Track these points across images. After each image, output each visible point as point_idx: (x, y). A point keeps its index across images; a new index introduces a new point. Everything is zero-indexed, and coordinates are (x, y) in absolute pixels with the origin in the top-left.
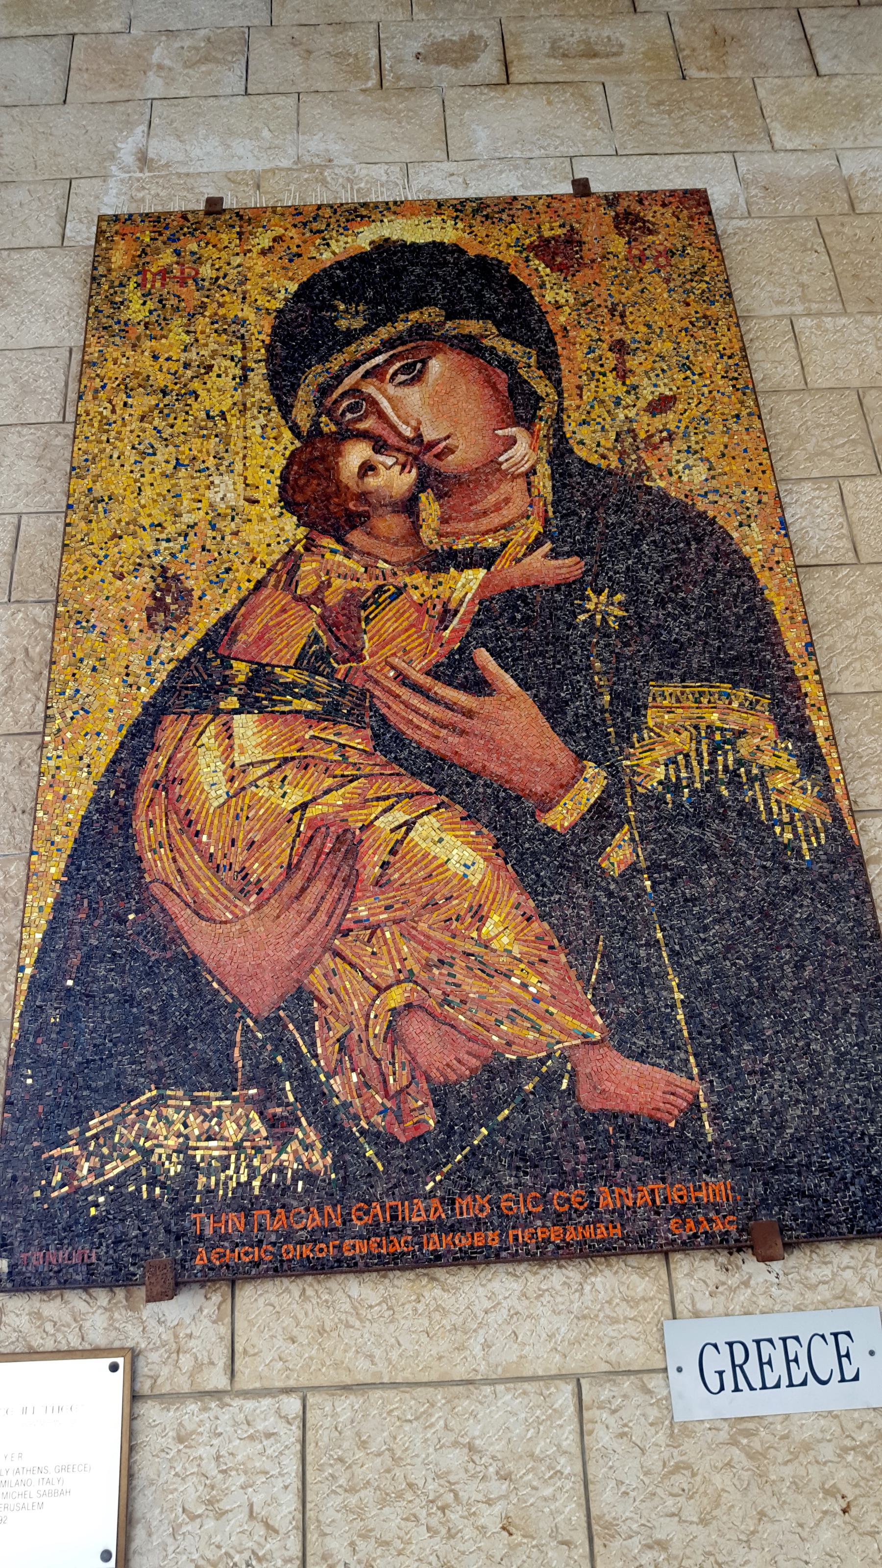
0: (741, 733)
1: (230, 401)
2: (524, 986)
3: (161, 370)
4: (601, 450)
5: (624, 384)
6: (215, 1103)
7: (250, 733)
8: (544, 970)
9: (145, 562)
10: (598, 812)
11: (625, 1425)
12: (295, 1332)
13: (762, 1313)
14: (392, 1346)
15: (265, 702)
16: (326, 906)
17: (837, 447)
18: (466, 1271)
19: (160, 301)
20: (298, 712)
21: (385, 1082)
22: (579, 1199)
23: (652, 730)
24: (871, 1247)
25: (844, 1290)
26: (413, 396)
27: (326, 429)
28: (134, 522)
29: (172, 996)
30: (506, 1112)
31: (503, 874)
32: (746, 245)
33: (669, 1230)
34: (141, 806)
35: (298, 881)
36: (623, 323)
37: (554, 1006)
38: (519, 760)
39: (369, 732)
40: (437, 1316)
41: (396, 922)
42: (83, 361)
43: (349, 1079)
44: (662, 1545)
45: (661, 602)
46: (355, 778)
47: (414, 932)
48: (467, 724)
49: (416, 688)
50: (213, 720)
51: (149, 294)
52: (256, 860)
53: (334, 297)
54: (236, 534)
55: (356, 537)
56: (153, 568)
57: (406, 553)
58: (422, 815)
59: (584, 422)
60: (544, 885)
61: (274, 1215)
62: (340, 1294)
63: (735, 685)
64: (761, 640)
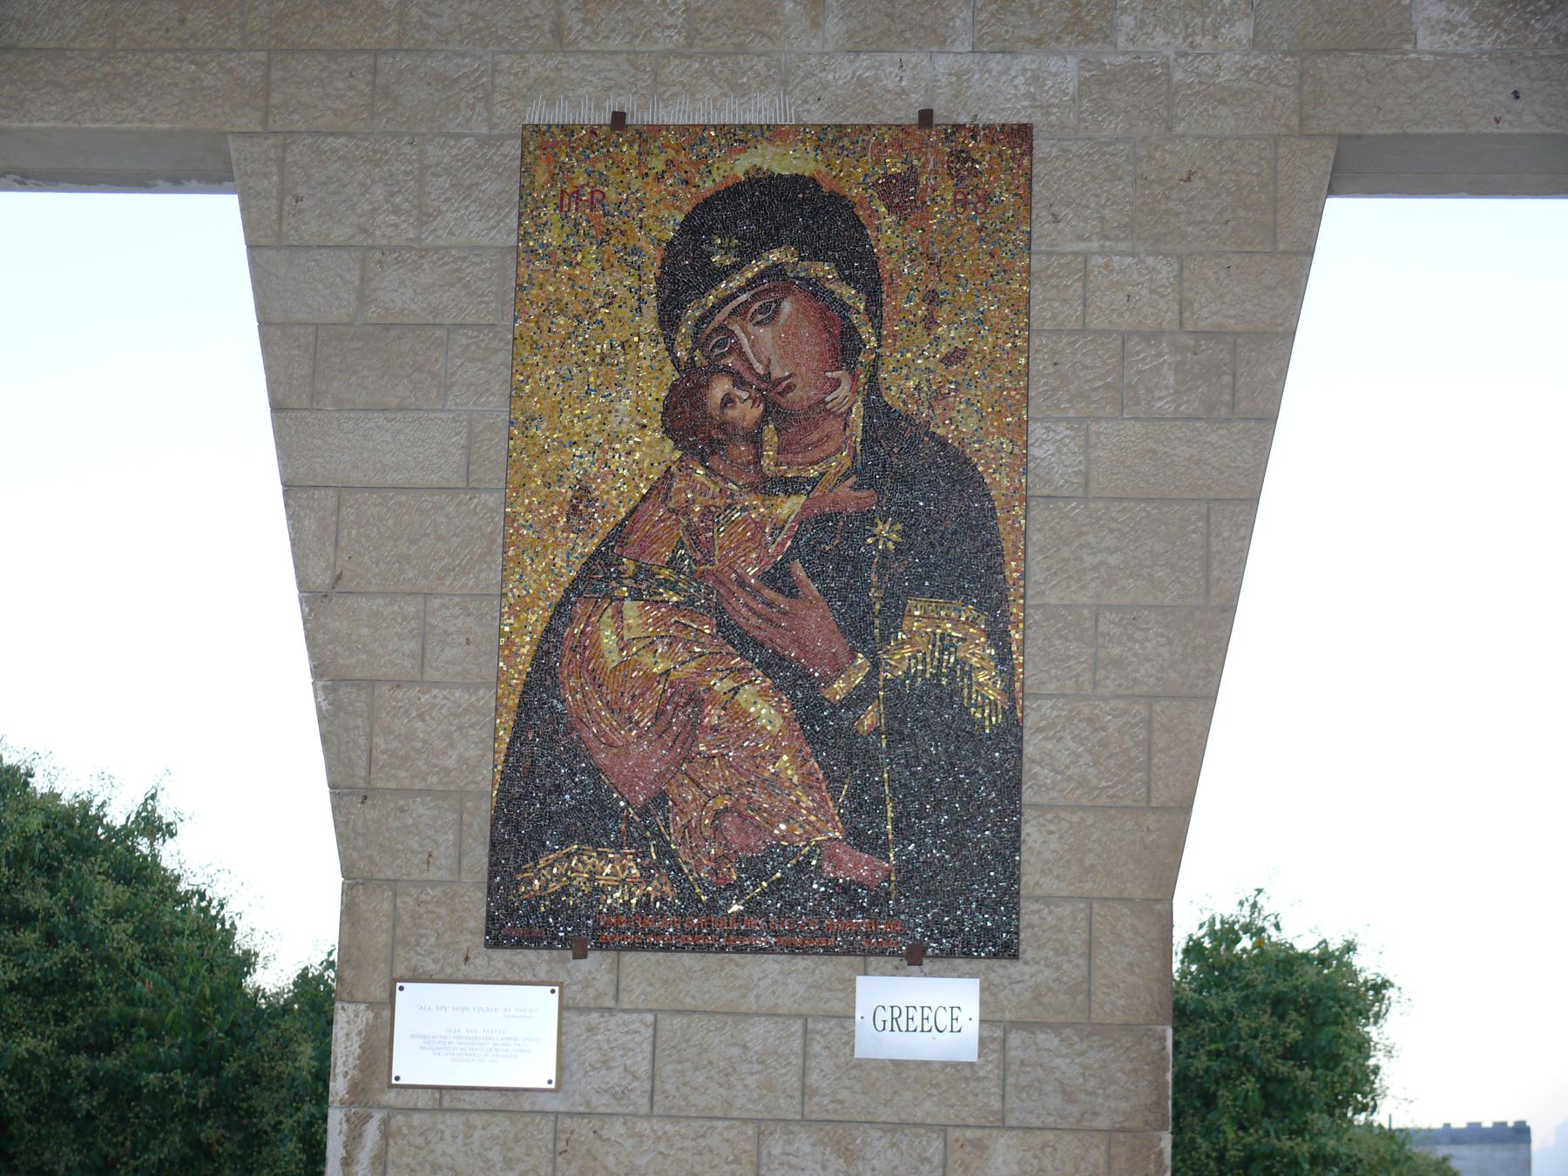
19: (575, 226)
27: (698, 364)
44: (840, 1102)
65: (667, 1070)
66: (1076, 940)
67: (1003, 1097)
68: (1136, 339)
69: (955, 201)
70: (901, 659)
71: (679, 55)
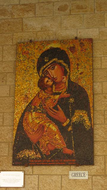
26: (53, 71)
35: (38, 131)
41: (48, 135)
48: (56, 114)
49: (51, 109)
55: (46, 91)
65: (40, 184)
66: (103, 162)
67: (92, 187)
69: (81, 50)
70: (74, 119)
71: (40, 31)
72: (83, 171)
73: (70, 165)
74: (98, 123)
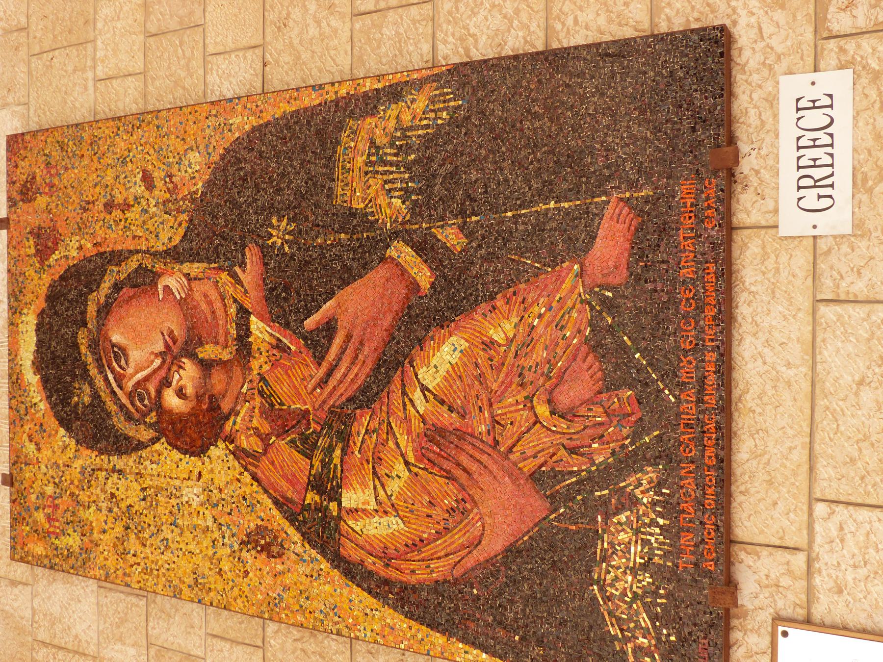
0: (372, 143)
1: (135, 484)
2: (540, 316)
3: (113, 529)
4: (176, 226)
5: (133, 206)
6: (606, 545)
7: (354, 496)
8: (530, 300)
9: (237, 554)
10: (422, 250)
11: (852, 269)
12: (769, 501)
13: (778, 163)
14: (784, 433)
15: (334, 483)
16: (477, 455)
17: (184, 55)
18: (735, 375)
19: (68, 524)
20: (342, 461)
21: (601, 424)
22: (687, 292)
23: (367, 205)
24: (738, 79)
25: (767, 100)
26: (136, 355)
27: (155, 419)
28: (211, 559)
29: (531, 569)
30: (625, 338)
31: (462, 324)
32: (46, 109)
33: (713, 229)
34: (400, 577)
35: (458, 473)
36: (93, 203)
37: (554, 297)
38: (383, 304)
39: (358, 411)
40: (765, 399)
41: (491, 405)
42: (105, 581)
43: (596, 449)
45: (279, 191)
46: (389, 424)
47: (498, 393)
48: (355, 339)
49: (330, 373)
50: (345, 521)
51: (63, 530)
52: (443, 501)
53: (69, 404)
54: (220, 490)
56: (241, 550)
57: (237, 372)
58: (417, 378)
59: (157, 236)
60: (471, 295)
61: (683, 511)
62: (745, 467)
63: (338, 143)
64: (308, 122)
68: (149, 25)
72: (776, 116)
73: (728, 228)
74: (426, 48)
